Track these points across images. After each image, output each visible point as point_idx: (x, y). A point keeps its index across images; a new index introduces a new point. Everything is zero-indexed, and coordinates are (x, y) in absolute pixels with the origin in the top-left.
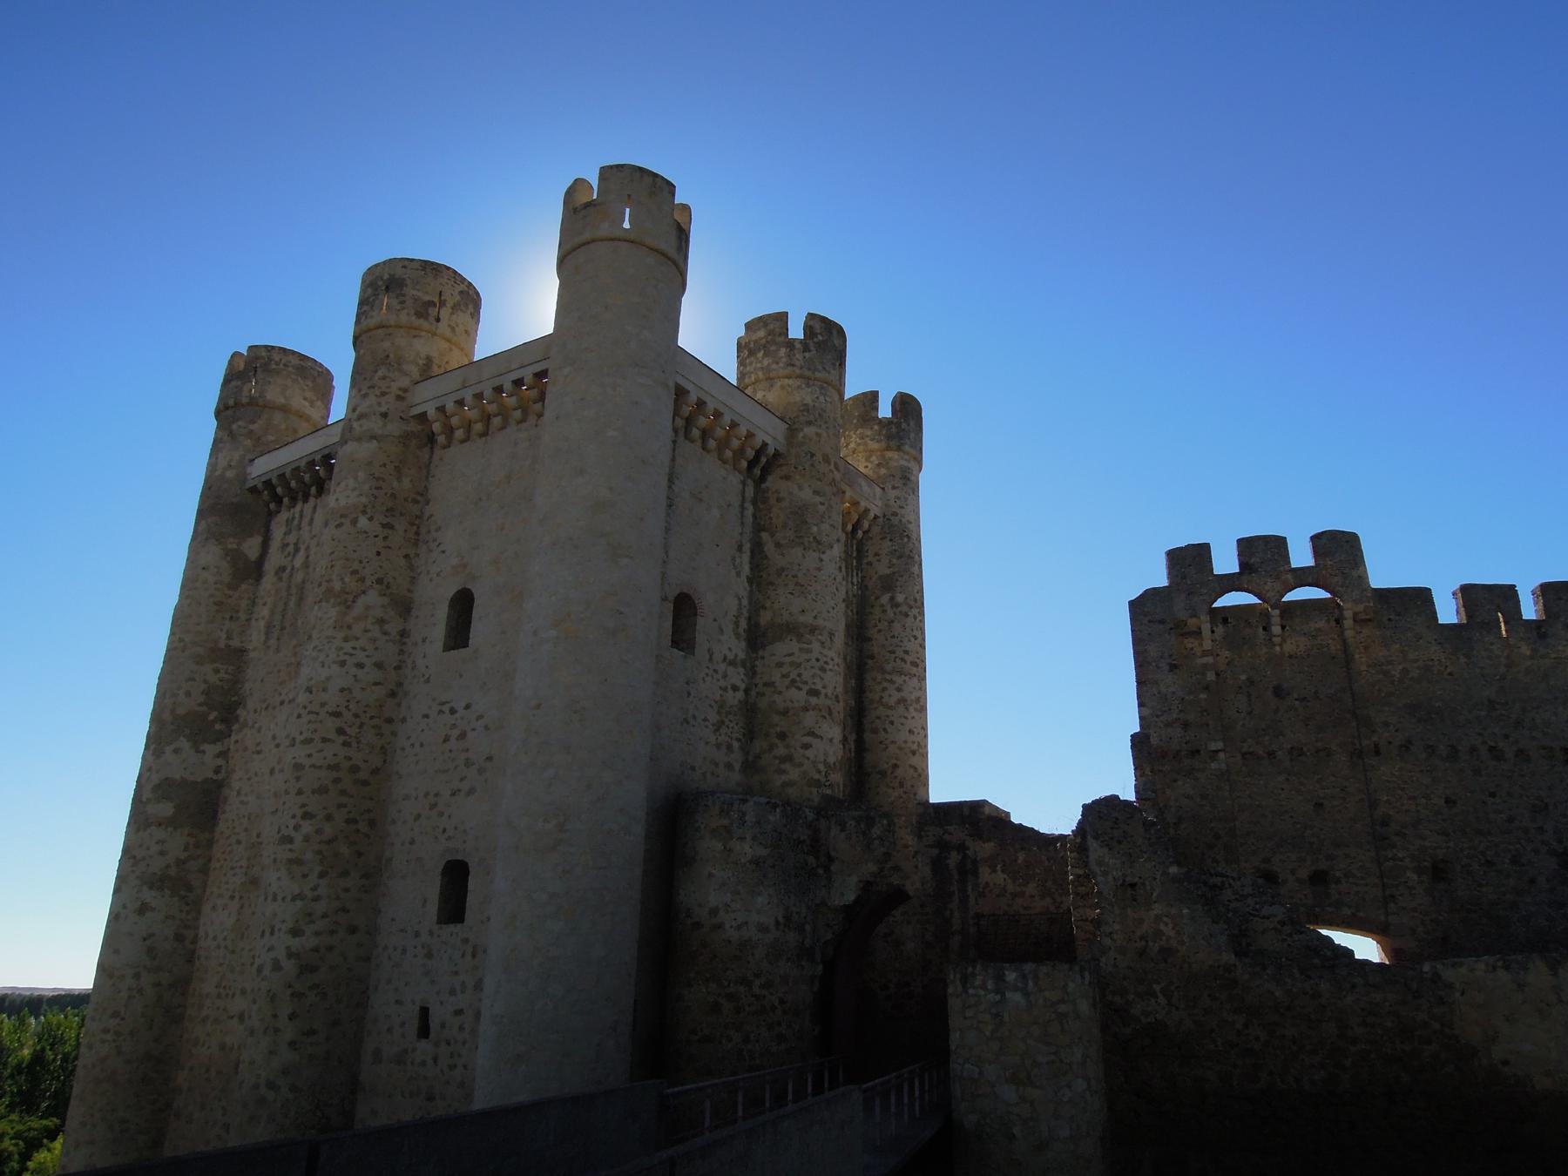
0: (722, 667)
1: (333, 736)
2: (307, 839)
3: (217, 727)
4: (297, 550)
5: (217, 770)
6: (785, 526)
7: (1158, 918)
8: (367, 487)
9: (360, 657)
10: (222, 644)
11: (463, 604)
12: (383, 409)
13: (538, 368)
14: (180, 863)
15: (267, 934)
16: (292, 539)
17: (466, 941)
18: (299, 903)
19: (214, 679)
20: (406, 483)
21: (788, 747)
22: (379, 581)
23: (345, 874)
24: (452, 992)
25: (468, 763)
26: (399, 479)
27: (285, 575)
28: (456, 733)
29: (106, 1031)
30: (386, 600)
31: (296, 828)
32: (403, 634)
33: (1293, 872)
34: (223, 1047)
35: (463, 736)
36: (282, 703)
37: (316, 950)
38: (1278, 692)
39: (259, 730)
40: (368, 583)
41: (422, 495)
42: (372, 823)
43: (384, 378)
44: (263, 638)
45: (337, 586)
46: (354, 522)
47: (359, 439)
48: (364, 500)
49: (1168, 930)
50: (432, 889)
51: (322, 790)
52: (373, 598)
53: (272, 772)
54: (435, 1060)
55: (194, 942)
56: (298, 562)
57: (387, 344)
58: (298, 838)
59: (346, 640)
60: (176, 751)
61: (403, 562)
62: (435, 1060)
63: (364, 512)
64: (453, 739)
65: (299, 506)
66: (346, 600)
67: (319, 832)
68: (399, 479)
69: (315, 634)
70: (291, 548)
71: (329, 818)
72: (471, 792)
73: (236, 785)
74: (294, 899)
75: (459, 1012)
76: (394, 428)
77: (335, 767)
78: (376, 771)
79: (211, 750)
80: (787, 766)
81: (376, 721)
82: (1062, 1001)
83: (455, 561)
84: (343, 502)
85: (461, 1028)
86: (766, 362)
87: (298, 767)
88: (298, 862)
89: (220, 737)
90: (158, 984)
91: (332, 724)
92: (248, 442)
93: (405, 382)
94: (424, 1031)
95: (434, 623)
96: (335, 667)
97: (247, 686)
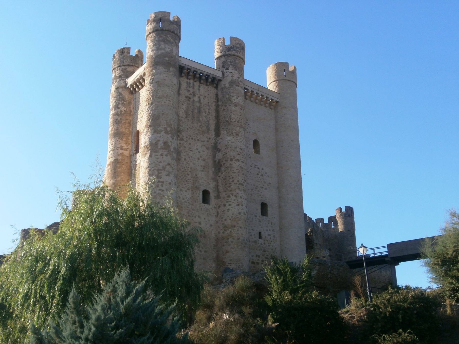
13: (278, 100)
28: (260, 174)
53: (198, 159)
62: (265, 244)
72: (266, 189)
75: (269, 235)
83: (254, 132)
94: (260, 237)
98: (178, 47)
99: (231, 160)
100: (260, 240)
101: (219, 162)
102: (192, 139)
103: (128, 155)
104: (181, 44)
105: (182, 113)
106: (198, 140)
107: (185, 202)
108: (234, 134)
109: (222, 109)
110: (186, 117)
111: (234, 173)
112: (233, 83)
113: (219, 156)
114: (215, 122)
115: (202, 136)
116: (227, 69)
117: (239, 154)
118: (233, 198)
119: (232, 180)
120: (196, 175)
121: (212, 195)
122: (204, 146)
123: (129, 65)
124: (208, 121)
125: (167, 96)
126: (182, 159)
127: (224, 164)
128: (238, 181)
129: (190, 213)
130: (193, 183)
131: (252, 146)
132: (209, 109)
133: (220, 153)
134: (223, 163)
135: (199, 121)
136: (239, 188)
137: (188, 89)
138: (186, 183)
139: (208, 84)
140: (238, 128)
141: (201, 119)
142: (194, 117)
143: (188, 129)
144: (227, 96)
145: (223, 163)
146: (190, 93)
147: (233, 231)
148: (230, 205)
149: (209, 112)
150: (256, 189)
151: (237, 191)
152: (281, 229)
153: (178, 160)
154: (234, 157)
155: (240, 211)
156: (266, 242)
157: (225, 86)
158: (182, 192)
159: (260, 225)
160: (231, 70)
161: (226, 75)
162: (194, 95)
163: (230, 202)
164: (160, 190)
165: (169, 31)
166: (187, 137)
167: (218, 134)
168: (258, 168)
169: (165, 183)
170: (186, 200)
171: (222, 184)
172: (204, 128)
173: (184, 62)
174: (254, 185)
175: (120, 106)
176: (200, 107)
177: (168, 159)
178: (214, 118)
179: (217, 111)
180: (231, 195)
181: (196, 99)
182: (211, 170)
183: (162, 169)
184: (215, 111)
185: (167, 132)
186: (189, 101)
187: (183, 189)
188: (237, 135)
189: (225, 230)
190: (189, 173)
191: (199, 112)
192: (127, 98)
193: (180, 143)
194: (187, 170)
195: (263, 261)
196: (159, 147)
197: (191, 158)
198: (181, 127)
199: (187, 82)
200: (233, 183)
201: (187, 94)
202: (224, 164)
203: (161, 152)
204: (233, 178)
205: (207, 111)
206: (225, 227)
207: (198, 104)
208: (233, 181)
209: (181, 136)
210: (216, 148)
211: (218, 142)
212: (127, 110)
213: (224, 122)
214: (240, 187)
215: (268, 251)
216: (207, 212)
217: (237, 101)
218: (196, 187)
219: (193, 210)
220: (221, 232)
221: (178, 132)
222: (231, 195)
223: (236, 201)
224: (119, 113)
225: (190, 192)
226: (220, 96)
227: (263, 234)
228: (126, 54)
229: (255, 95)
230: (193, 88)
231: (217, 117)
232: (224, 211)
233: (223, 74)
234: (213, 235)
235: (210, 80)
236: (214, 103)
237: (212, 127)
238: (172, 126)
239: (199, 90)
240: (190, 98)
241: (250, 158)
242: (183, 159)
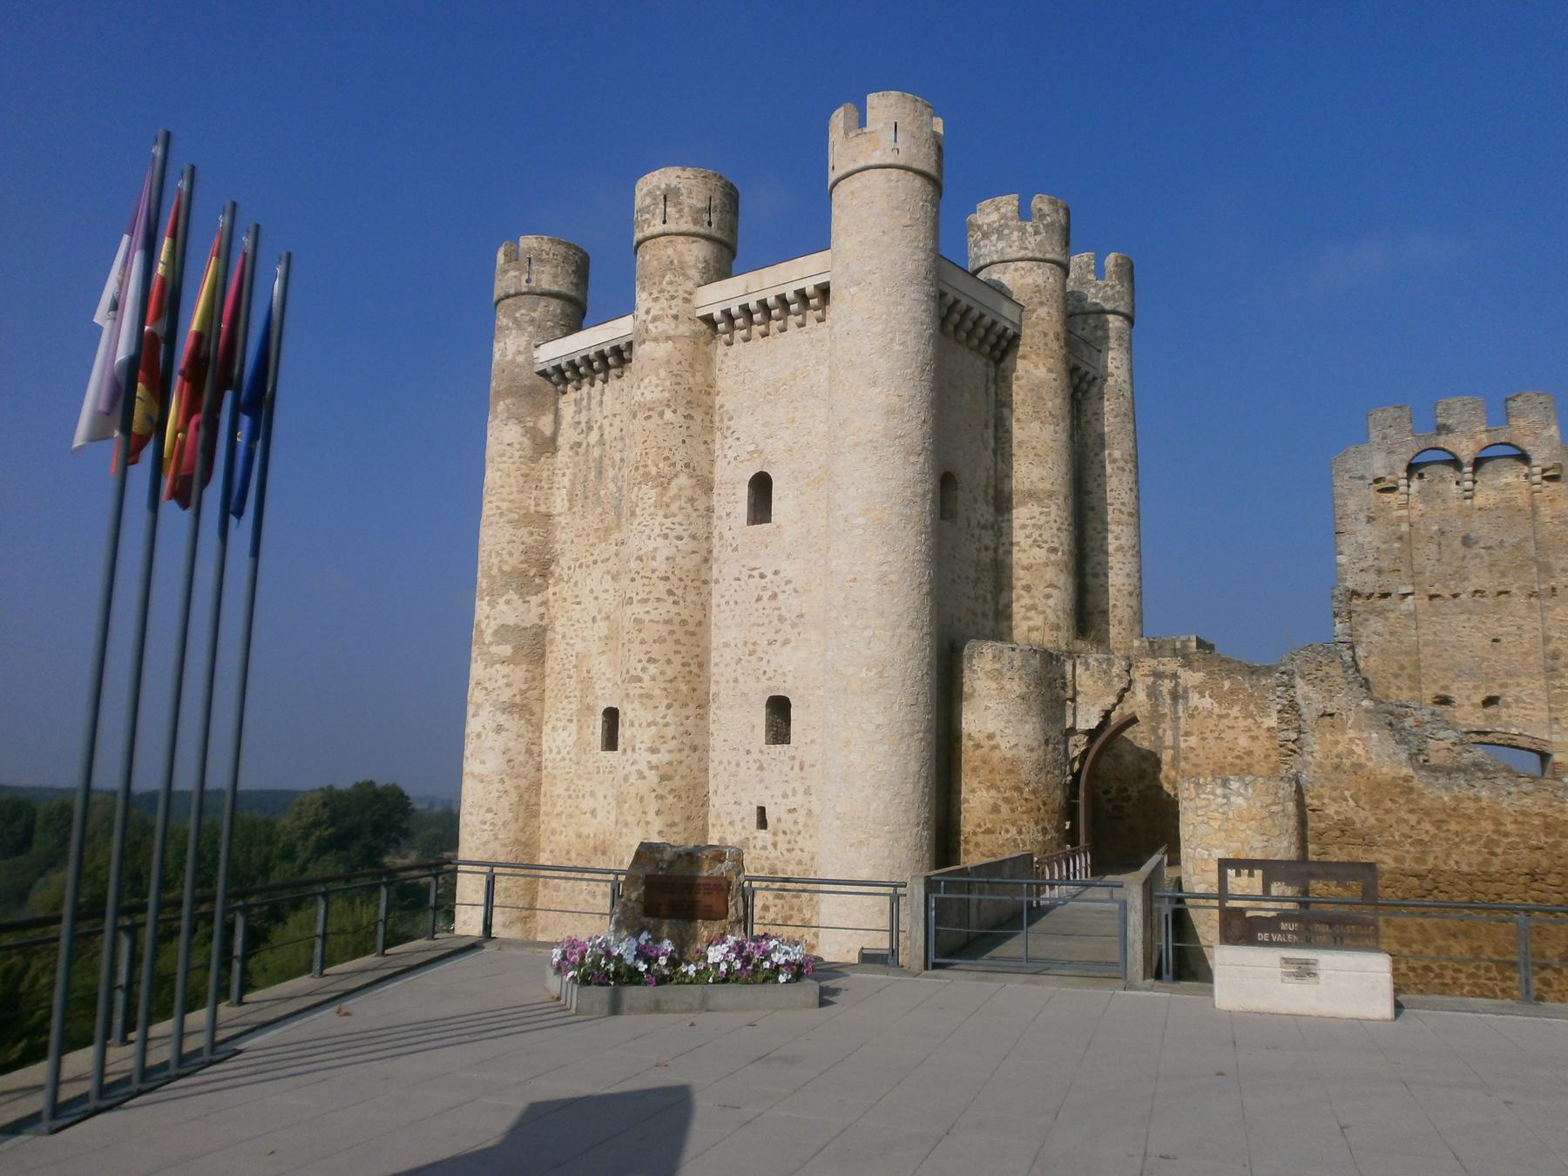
0: (977, 531)
1: (665, 596)
2: (653, 679)
3: (537, 580)
4: (590, 428)
5: (542, 617)
6: (1024, 402)
7: (1351, 740)
8: (668, 383)
9: (679, 530)
10: (532, 509)
11: (761, 486)
12: (674, 311)
13: (820, 280)
14: (523, 692)
15: (629, 751)
16: (583, 418)
18: (654, 729)
19: (529, 540)
20: (699, 378)
21: (1032, 597)
22: (687, 466)
23: (685, 705)
24: (785, 796)
25: (781, 619)
26: (694, 376)
27: (582, 450)
28: (766, 595)
30: (694, 481)
31: (644, 670)
32: (710, 510)
33: (1468, 698)
34: (579, 836)
36: (595, 562)
37: (670, 763)
38: (1466, 541)
39: (576, 584)
40: (678, 467)
41: (709, 388)
42: (700, 665)
43: (671, 283)
44: (567, 505)
45: (654, 471)
46: (661, 414)
47: (656, 340)
48: (667, 395)
49: (1359, 750)
50: (760, 717)
51: (662, 640)
52: (683, 480)
53: (594, 619)
54: (775, 845)
55: (540, 755)
56: (594, 436)
57: (670, 251)
58: (646, 678)
59: (666, 517)
60: (508, 602)
61: (702, 448)
62: (775, 845)
63: (669, 406)
64: (765, 598)
65: (585, 388)
66: (663, 483)
67: (662, 673)
68: (694, 376)
69: (638, 511)
70: (583, 425)
71: (669, 662)
72: (786, 642)
73: (559, 629)
74: (649, 725)
76: (684, 329)
77: (668, 622)
78: (700, 624)
79: (534, 600)
80: (1032, 613)
81: (697, 584)
82: (1274, 803)
83: (751, 448)
84: (649, 397)
85: (795, 822)
86: (1000, 245)
87: (638, 621)
88: (650, 697)
89: (539, 589)
90: (518, 787)
91: (662, 587)
92: (530, 329)
93: (689, 285)
94: (762, 823)
95: (734, 500)
96: (660, 540)
97: (557, 546)
124: (620, 490)
159: (761, 781)
168: (762, 576)
172: (610, 517)
181: (594, 436)
187: (559, 724)
225: (573, 727)
227: (771, 818)
238: (495, 571)
241: (736, 549)
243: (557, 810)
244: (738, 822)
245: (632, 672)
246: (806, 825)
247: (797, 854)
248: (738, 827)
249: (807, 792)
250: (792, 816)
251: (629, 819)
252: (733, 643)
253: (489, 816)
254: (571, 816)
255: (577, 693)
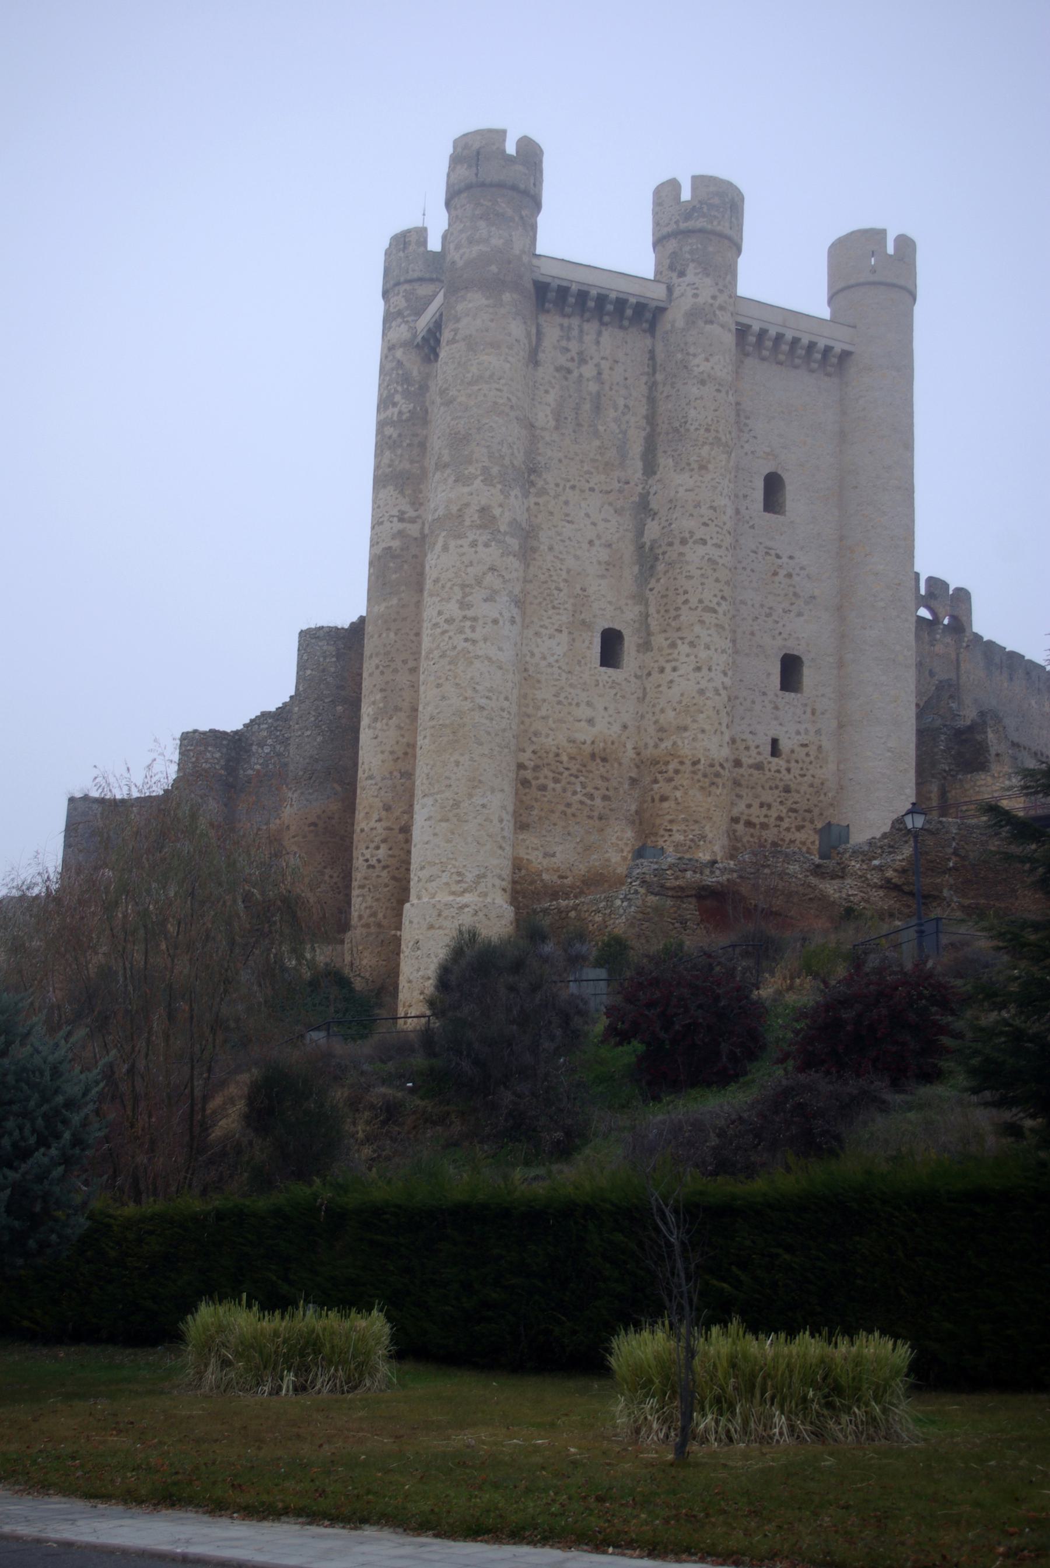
13: (847, 347)
17: (806, 705)
24: (798, 733)
25: (795, 594)
29: (503, 710)
31: (718, 604)
35: (789, 576)
53: (591, 543)
54: (788, 770)
58: (720, 610)
62: (788, 770)
72: (800, 614)
83: (768, 450)
85: (807, 755)
98: (532, 229)
99: (684, 542)
100: (775, 760)
101: (651, 549)
102: (573, 487)
103: (416, 534)
104: (544, 221)
105: (543, 416)
106: (592, 490)
107: (550, 665)
108: (695, 466)
109: (665, 394)
110: (557, 428)
111: (690, 577)
112: (694, 315)
113: (652, 530)
114: (643, 434)
115: (603, 477)
116: (682, 274)
117: (705, 524)
118: (683, 648)
119: (682, 598)
120: (584, 590)
121: (630, 642)
122: (610, 504)
123: (420, 280)
124: (625, 433)
125: (492, 376)
126: (542, 547)
127: (664, 553)
128: (701, 601)
129: (563, 695)
130: (575, 611)
131: (759, 495)
132: (626, 398)
133: (656, 522)
134: (660, 551)
135: (596, 434)
136: (702, 622)
137: (564, 343)
138: (550, 612)
139: (626, 323)
140: (707, 448)
141: (601, 428)
142: (579, 425)
143: (560, 461)
144: (679, 356)
145: (660, 551)
146: (569, 356)
147: (680, 743)
148: (674, 669)
149: (626, 406)
150: (768, 615)
151: (697, 629)
152: (841, 726)
153: (527, 553)
154: (692, 533)
155: (704, 684)
156: (793, 764)
157: (673, 326)
158: (539, 640)
159: (776, 718)
160: (690, 277)
161: (677, 293)
162: (583, 360)
163: (676, 660)
164: (466, 640)
165: (500, 185)
166: (557, 485)
167: (650, 468)
169: (481, 622)
170: (551, 660)
171: (658, 612)
173: (548, 271)
174: (762, 606)
175: (398, 398)
176: (598, 394)
177: (491, 554)
178: (643, 423)
179: (652, 401)
180: (679, 642)
181: (588, 371)
182: (630, 571)
183: (473, 582)
184: (644, 400)
185: (488, 481)
186: (566, 379)
187: (544, 631)
188: (703, 467)
189: (661, 740)
190: (562, 585)
191: (597, 408)
192: (415, 373)
193: (537, 504)
194: (555, 578)
195: (780, 818)
196: (467, 523)
197: (567, 543)
198: (539, 458)
199: (562, 326)
200: (685, 608)
201: (562, 360)
202: (664, 553)
203: (471, 537)
204: (686, 592)
205: (621, 402)
206: (661, 730)
207: (593, 387)
208: (686, 602)
209: (540, 483)
210: (644, 508)
211: (652, 491)
212: (414, 407)
213: (667, 434)
214: (708, 617)
215: (798, 792)
216: (613, 691)
217: (705, 367)
218: (583, 622)
219: (571, 685)
220: (651, 743)
221: (528, 475)
222: (679, 642)
223: (693, 657)
224: (395, 418)
225: (564, 637)
226: (660, 356)
227: (785, 745)
228: (412, 248)
229: (766, 341)
230: (581, 341)
231: (651, 419)
232: (659, 686)
233: (670, 290)
234: (631, 753)
235: (629, 312)
236: (644, 378)
237: (636, 448)
238: (507, 462)
239: (598, 343)
240: (569, 371)
241: (753, 527)
242: (544, 548)
243: (543, 712)
244: (753, 748)
245: (707, 603)
246: (817, 758)
247: (808, 779)
248: (753, 752)
249: (818, 732)
250: (805, 750)
251: (707, 727)
252: (750, 603)
253: (506, 704)
254: (561, 721)
255: (568, 606)
